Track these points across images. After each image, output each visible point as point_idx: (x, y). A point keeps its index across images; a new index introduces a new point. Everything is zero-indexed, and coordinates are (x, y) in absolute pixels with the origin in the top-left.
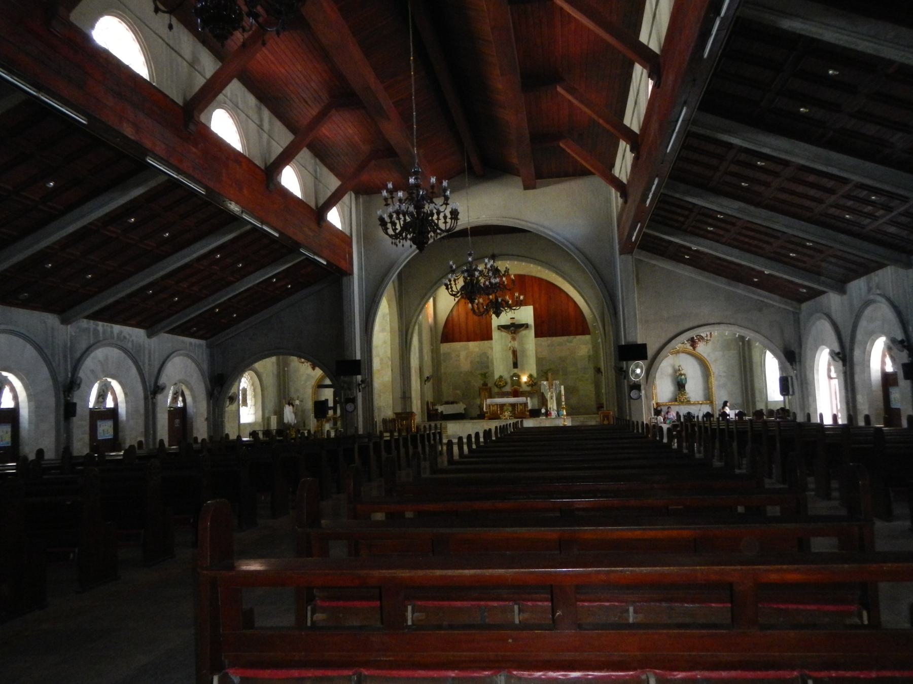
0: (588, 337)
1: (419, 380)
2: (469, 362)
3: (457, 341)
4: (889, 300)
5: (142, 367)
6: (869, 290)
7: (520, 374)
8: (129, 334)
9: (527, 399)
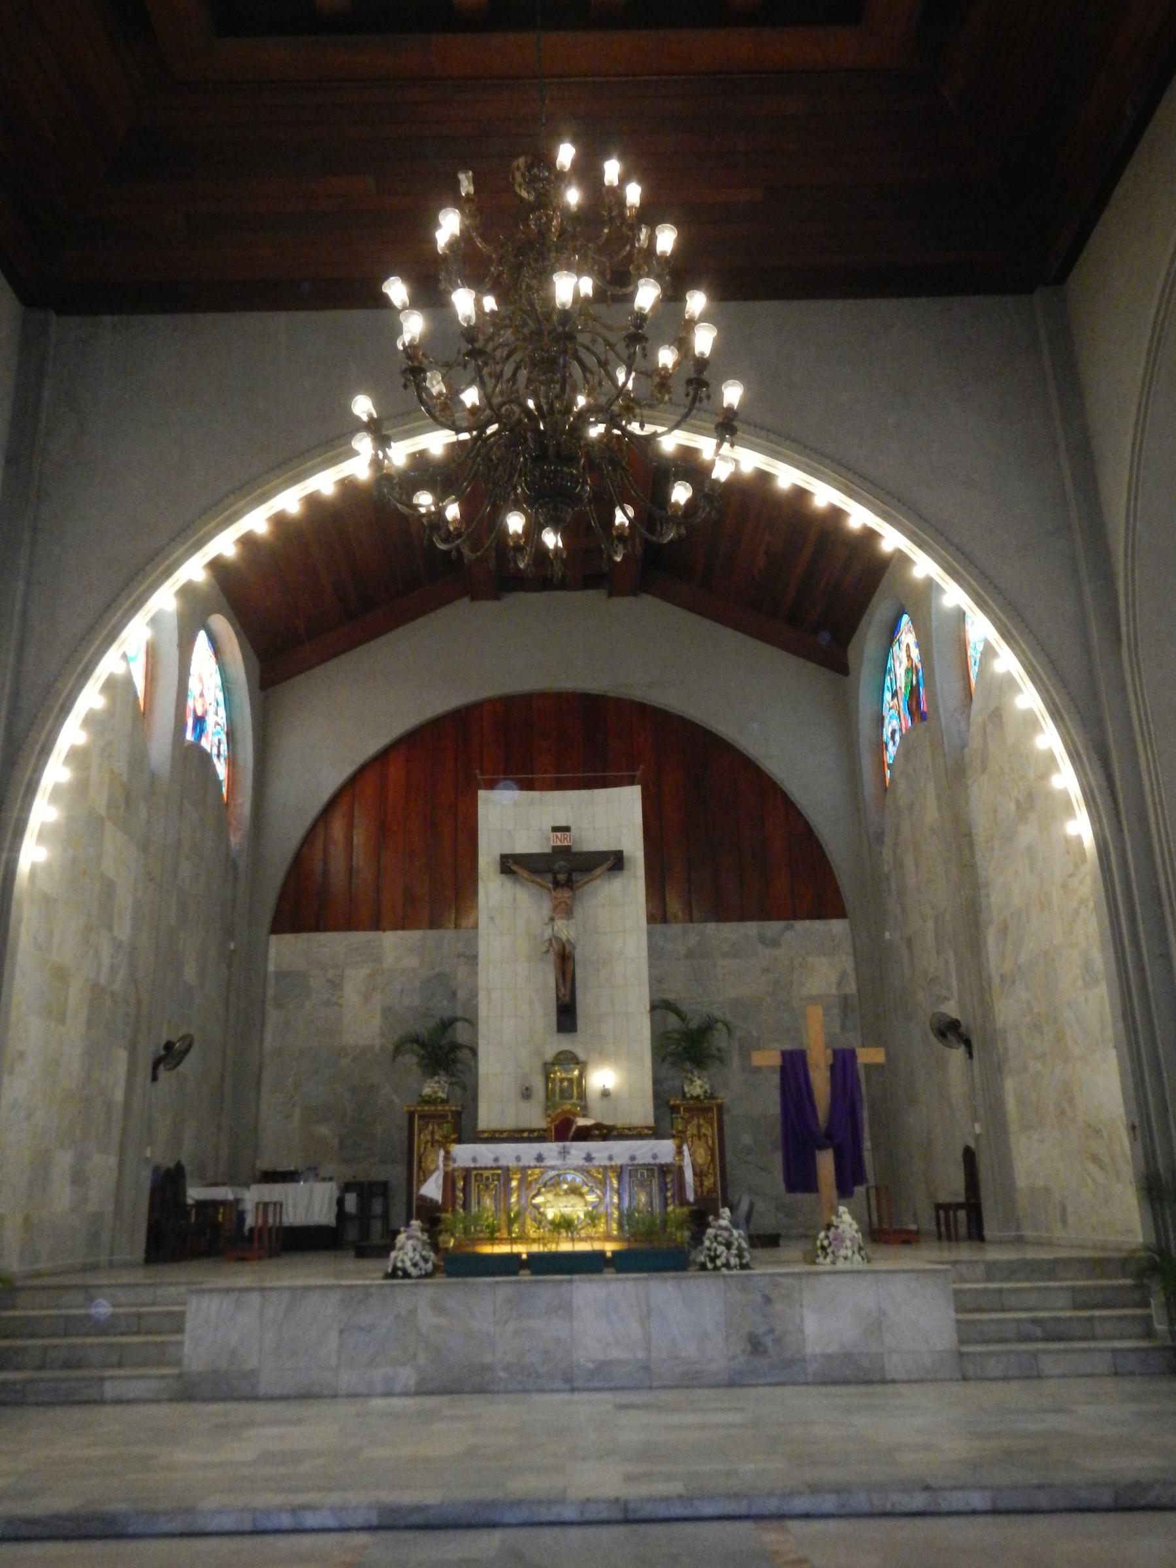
0: (838, 926)
1: (123, 1055)
7: (582, 1056)
9: (680, 1152)
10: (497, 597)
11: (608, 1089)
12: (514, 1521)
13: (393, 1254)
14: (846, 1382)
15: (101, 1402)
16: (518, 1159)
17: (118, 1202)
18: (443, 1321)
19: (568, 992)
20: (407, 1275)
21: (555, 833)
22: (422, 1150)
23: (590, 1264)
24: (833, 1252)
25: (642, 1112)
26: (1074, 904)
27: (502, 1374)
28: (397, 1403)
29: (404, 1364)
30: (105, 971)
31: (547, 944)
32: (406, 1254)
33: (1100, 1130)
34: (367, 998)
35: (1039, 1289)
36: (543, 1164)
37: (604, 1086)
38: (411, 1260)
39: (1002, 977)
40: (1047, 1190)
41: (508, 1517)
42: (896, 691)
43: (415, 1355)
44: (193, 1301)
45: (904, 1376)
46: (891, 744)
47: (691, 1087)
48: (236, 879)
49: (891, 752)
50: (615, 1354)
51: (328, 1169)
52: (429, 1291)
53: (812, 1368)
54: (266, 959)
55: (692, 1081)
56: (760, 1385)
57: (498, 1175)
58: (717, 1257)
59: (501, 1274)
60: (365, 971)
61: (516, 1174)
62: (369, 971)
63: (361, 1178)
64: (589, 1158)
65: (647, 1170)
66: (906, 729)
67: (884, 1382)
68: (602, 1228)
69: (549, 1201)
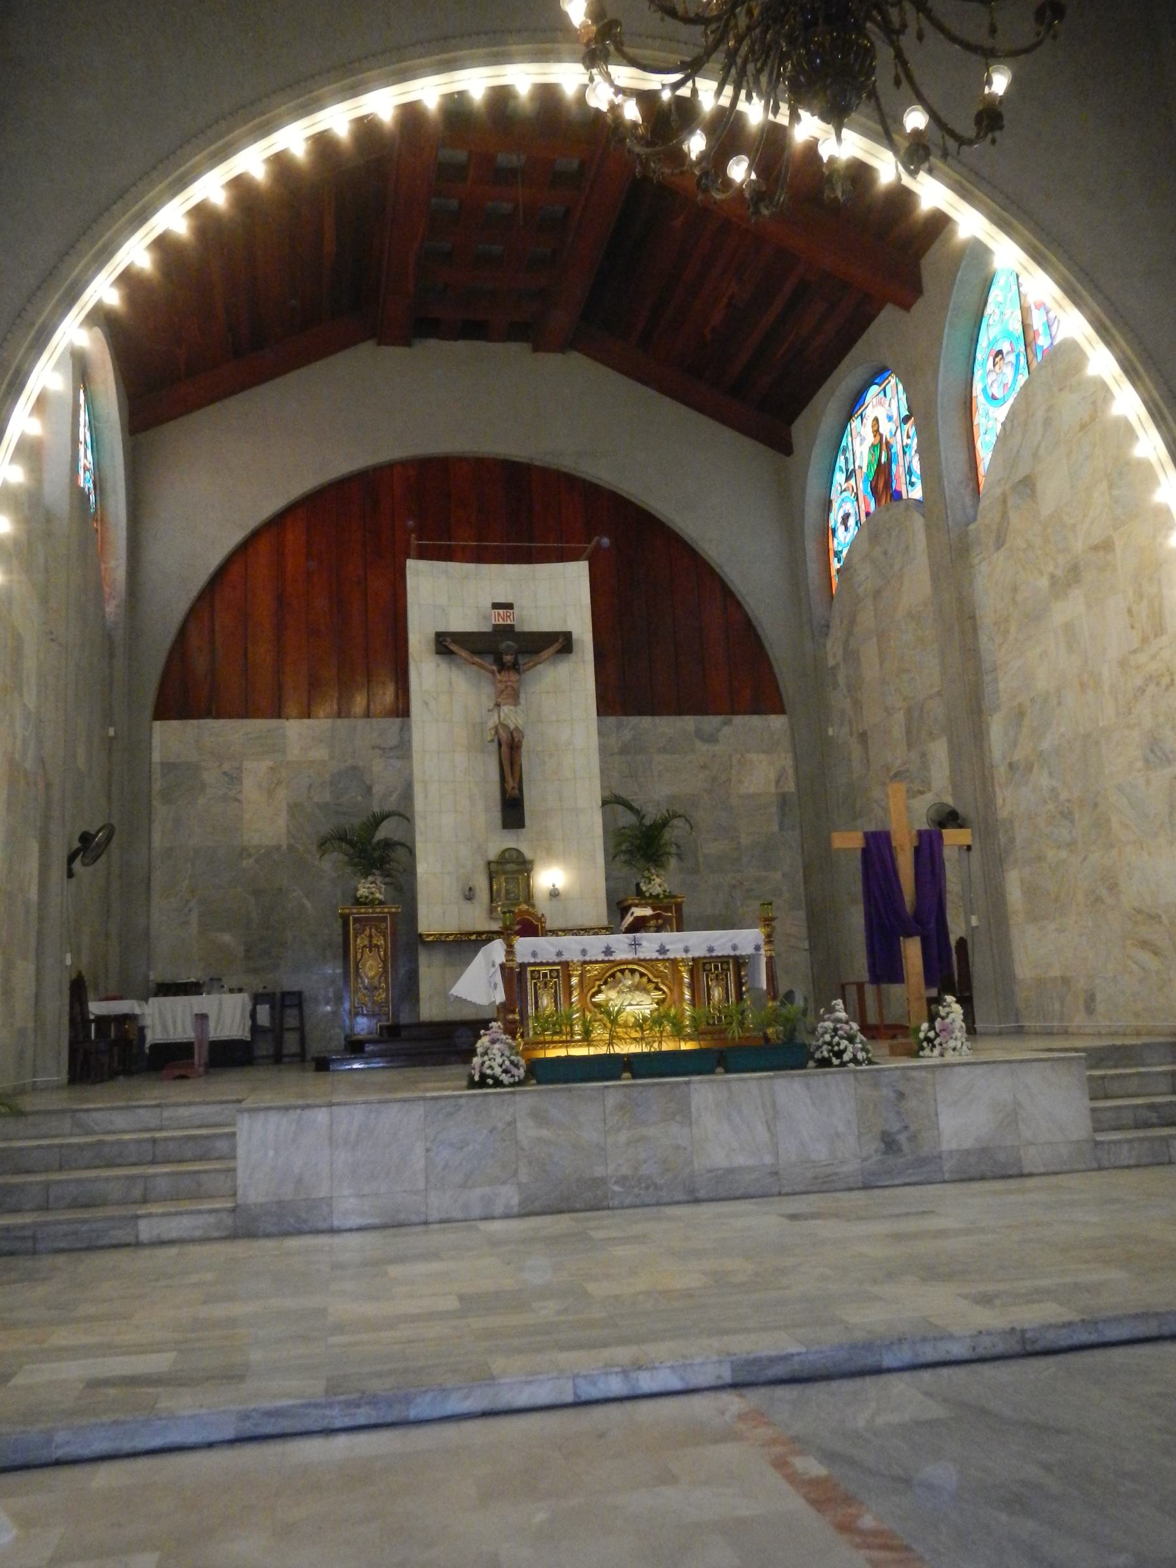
0: (777, 722)
1: (34, 846)
2: (284, 805)
7: (528, 855)
10: (408, 344)
11: (557, 889)
12: (896, 1364)
13: (476, 1060)
14: (982, 1178)
15: (138, 1245)
16: (584, 952)
17: (38, 1017)
18: (545, 1133)
19: (516, 786)
20: (498, 1083)
21: (496, 611)
22: (359, 956)
24: (941, 1044)
25: (596, 911)
26: (1139, 682)
27: (617, 1188)
28: (496, 1226)
29: (504, 1183)
30: (19, 742)
31: (493, 732)
32: (495, 1059)
33: (1159, 917)
34: (270, 793)
35: (1140, 1074)
36: (612, 958)
37: (554, 886)
38: (501, 1066)
39: (1011, 765)
40: (1066, 981)
41: (888, 1361)
42: (854, 471)
43: (515, 1173)
44: (244, 1125)
45: (1042, 1170)
46: (841, 529)
47: (650, 886)
48: (112, 655)
49: (842, 540)
50: (740, 1160)
51: (230, 981)
53: (948, 1166)
54: (150, 749)
55: (650, 881)
56: (898, 1186)
57: (557, 971)
58: (844, 1051)
59: (607, 1079)
60: (266, 764)
61: (577, 970)
62: (271, 764)
63: (269, 990)
64: (662, 950)
65: (722, 963)
66: (868, 514)
67: (1022, 1175)
69: (611, 999)
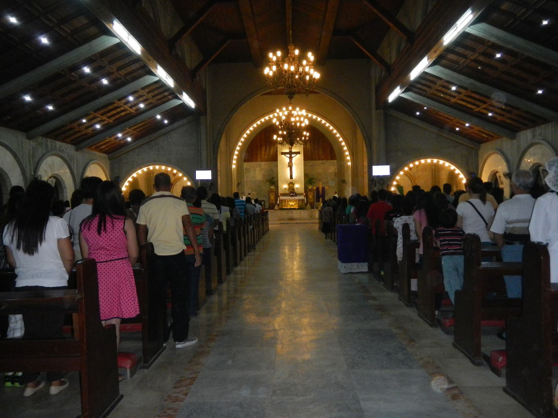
0: (335, 161)
3: (254, 161)
4: (549, 143)
5: (73, 170)
6: (534, 136)
8: (65, 148)
9: (304, 198)
23: (295, 209)
25: (302, 191)
52: (279, 212)
64: (295, 198)
68: (296, 206)
